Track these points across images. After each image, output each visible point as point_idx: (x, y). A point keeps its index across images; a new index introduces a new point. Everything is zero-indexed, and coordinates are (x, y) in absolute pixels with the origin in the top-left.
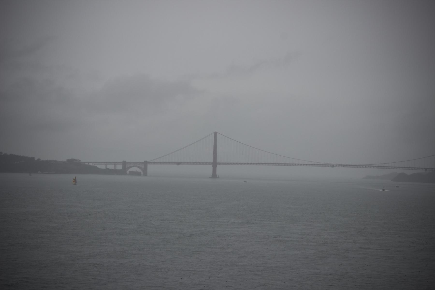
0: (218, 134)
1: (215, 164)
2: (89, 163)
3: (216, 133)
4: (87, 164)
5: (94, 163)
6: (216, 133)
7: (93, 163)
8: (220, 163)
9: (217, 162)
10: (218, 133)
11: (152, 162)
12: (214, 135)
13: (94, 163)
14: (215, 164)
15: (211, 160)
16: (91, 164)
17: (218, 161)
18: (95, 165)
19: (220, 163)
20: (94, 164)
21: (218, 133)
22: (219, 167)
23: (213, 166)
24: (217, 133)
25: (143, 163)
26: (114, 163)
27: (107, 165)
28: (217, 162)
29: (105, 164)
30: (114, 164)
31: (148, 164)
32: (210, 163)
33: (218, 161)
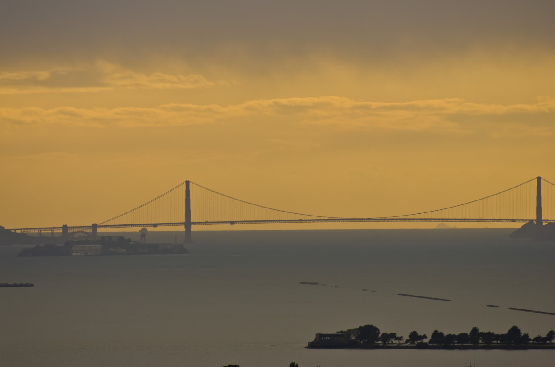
1: (188, 223)
2: (16, 230)
3: (187, 183)
4: (14, 231)
5: (23, 230)
6: (187, 183)
7: (21, 229)
10: (193, 183)
12: (184, 185)
13: (23, 230)
14: (188, 223)
15: (184, 221)
17: (193, 220)
18: (24, 232)
21: (193, 183)
22: (194, 228)
23: (185, 227)
24: (190, 183)
25: (90, 227)
26: (51, 228)
27: (41, 231)
29: (38, 231)
30: (51, 230)
31: (98, 228)
32: (181, 224)
33: (192, 221)
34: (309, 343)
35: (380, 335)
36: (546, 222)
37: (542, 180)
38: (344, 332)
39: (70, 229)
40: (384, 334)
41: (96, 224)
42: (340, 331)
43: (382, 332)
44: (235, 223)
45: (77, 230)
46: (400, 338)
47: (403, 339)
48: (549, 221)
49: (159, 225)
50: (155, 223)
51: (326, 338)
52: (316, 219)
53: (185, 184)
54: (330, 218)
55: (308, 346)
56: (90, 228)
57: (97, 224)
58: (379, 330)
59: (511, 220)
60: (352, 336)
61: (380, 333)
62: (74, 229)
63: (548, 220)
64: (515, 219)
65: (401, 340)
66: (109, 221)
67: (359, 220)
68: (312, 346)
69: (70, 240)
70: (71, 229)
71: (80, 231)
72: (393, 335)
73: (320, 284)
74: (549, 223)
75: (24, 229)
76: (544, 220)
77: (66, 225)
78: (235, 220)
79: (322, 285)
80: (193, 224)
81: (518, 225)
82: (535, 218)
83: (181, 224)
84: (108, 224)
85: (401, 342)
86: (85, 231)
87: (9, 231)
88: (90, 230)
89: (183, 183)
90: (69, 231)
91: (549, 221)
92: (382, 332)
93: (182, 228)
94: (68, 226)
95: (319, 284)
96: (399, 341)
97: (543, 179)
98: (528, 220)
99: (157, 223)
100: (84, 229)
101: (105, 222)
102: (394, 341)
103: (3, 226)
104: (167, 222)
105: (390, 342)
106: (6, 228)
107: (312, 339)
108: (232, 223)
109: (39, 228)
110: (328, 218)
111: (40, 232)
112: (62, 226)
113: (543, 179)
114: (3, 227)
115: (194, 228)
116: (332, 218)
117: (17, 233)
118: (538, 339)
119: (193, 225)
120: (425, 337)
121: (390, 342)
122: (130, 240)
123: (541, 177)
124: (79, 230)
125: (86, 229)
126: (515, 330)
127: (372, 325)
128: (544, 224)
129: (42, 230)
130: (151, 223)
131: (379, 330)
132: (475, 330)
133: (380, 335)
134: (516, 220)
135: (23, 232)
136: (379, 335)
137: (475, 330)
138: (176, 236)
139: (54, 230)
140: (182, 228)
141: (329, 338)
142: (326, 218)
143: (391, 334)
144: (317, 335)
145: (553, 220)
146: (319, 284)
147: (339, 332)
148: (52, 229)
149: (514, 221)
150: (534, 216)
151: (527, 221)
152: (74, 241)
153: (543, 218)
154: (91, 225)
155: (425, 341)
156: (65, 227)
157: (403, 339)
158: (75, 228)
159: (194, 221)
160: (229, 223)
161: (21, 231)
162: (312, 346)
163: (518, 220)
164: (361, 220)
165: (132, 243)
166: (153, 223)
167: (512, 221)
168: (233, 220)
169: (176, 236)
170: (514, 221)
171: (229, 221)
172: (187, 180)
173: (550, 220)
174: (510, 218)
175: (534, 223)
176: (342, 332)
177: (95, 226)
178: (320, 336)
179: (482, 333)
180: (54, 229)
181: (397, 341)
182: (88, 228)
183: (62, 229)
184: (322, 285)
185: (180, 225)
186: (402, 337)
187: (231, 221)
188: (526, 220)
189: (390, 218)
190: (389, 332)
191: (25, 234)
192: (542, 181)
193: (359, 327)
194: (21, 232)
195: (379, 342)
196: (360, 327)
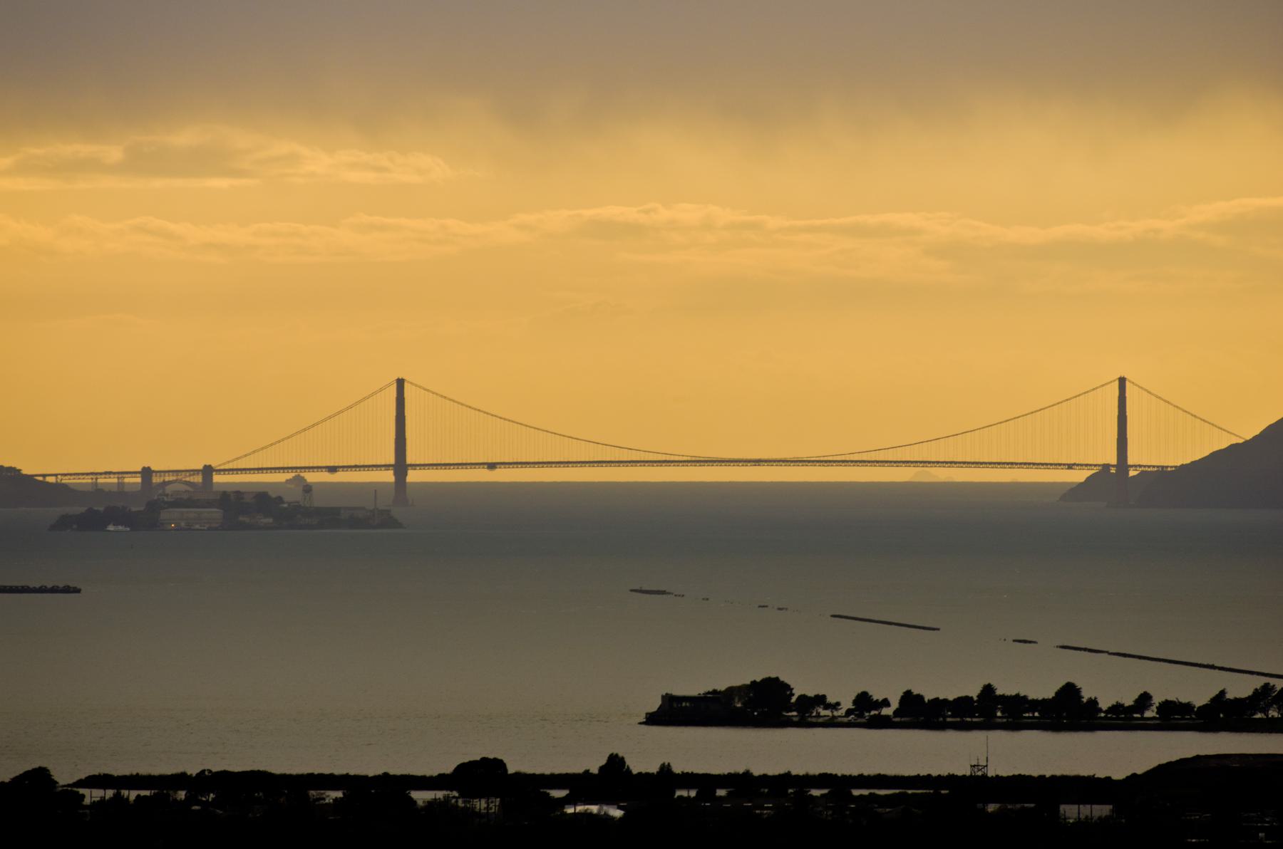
0: (407, 386)
1: (401, 466)
2: (44, 476)
3: (400, 383)
4: (41, 478)
5: (59, 477)
6: (400, 383)
7: (56, 475)
8: (414, 466)
9: (1129, 464)
10: (411, 383)
11: (227, 467)
12: (394, 388)
13: (59, 477)
14: (401, 466)
15: (392, 460)
16: (51, 480)
18: (63, 481)
19: (414, 466)
20: (61, 480)
21: (411, 383)
22: (413, 476)
23: (395, 474)
26: (118, 473)
27: (97, 479)
28: (1129, 464)
29: (92, 479)
30: (118, 478)
31: (214, 473)
32: (387, 467)
33: (409, 461)
34: (647, 714)
35: (794, 699)
36: (1136, 470)
37: (1127, 383)
38: (720, 692)
39: (156, 476)
40: (802, 698)
41: (210, 466)
42: (711, 690)
43: (797, 692)
44: (498, 466)
45: (172, 478)
46: (836, 706)
47: (840, 707)
48: (1143, 469)
49: (341, 470)
50: (332, 464)
51: (684, 704)
52: (664, 459)
53: (395, 385)
54: (693, 459)
55: (645, 720)
56: (198, 474)
57: (213, 466)
58: (793, 689)
59: (1064, 465)
60: (736, 700)
61: (793, 695)
62: (165, 476)
63: (1140, 466)
64: (1072, 462)
65: (837, 710)
66: (238, 459)
67: (753, 464)
68: (653, 719)
69: (156, 498)
70: (158, 474)
71: (177, 480)
72: (820, 700)
73: (672, 594)
74: (1142, 471)
75: (62, 475)
76: (1132, 466)
77: (149, 468)
78: (498, 461)
79: (676, 595)
80: (410, 468)
81: (1080, 476)
82: (1114, 461)
83: (387, 467)
84: (235, 467)
85: (836, 713)
86: (188, 479)
87: (30, 478)
88: (198, 479)
89: (390, 385)
90: (156, 480)
91: (1143, 469)
92: (797, 692)
93: (388, 477)
94: (153, 469)
95: (669, 593)
96: (832, 712)
97: (1130, 381)
98: (1099, 465)
99: (336, 465)
100: (186, 476)
101: (229, 462)
102: (823, 712)
103: (18, 468)
104: (358, 464)
105: (814, 714)
106: (25, 472)
107: (654, 705)
108: (492, 466)
109: (92, 474)
110: (689, 459)
111: (94, 480)
112: (140, 470)
113: (1130, 381)
114: (20, 470)
115: (413, 476)
116: (698, 459)
117: (48, 483)
118: (1117, 709)
119: (412, 469)
120: (886, 703)
121: (814, 714)
122: (280, 499)
123: (1126, 376)
124: (174, 478)
125: (190, 475)
126: (1070, 691)
127: (777, 679)
128: (1132, 473)
129: (99, 477)
130: (324, 465)
131: (793, 689)
132: (988, 690)
133: (794, 699)
134: (1074, 464)
135: (61, 480)
136: (791, 699)
137: (988, 690)
138: (376, 491)
139: (124, 478)
140: (388, 477)
141: (688, 704)
142: (685, 458)
143: (817, 696)
144: (663, 697)
145: (1149, 467)
146: (669, 593)
147: (709, 693)
148: (120, 476)
149: (1070, 466)
150: (1112, 459)
151: (1097, 468)
152: (166, 499)
153: (1130, 462)
154: (201, 467)
155: (886, 711)
156: (147, 472)
157: (841, 708)
158: (167, 474)
159: (413, 463)
160: (486, 467)
161: (57, 479)
162: (653, 719)
163: (1078, 465)
164: (758, 462)
165: (286, 505)
166: (328, 464)
167: (1067, 467)
168: (494, 461)
169: (376, 491)
170: (1070, 466)
171: (485, 461)
172: (400, 378)
173: (1145, 466)
174: (1063, 462)
175: (1112, 471)
176: (715, 692)
177: (208, 471)
178: (669, 700)
179: (1003, 696)
180: (125, 475)
181: (828, 713)
182: (194, 475)
183: (139, 475)
184: (676, 595)
185: (385, 470)
186: (838, 704)
187: (490, 461)
188: (1095, 465)
189: (817, 459)
190: (811, 694)
191: (65, 485)
192: (1128, 385)
193: (752, 682)
194: (57, 481)
195: (790, 714)
196: (754, 683)
